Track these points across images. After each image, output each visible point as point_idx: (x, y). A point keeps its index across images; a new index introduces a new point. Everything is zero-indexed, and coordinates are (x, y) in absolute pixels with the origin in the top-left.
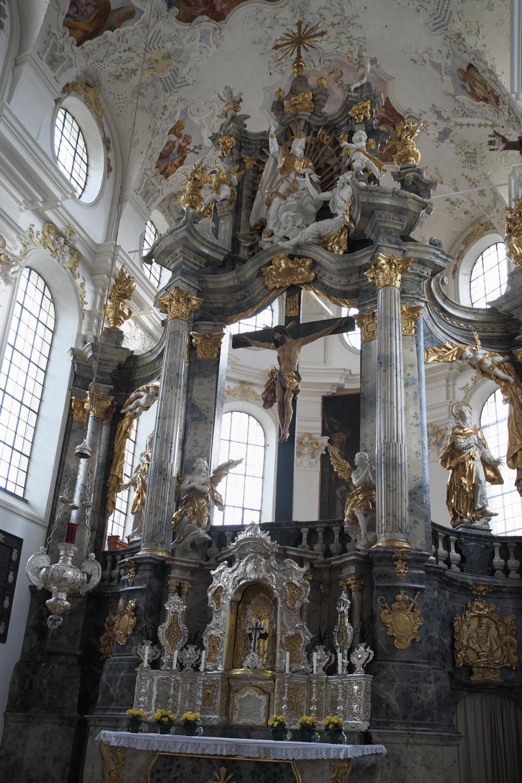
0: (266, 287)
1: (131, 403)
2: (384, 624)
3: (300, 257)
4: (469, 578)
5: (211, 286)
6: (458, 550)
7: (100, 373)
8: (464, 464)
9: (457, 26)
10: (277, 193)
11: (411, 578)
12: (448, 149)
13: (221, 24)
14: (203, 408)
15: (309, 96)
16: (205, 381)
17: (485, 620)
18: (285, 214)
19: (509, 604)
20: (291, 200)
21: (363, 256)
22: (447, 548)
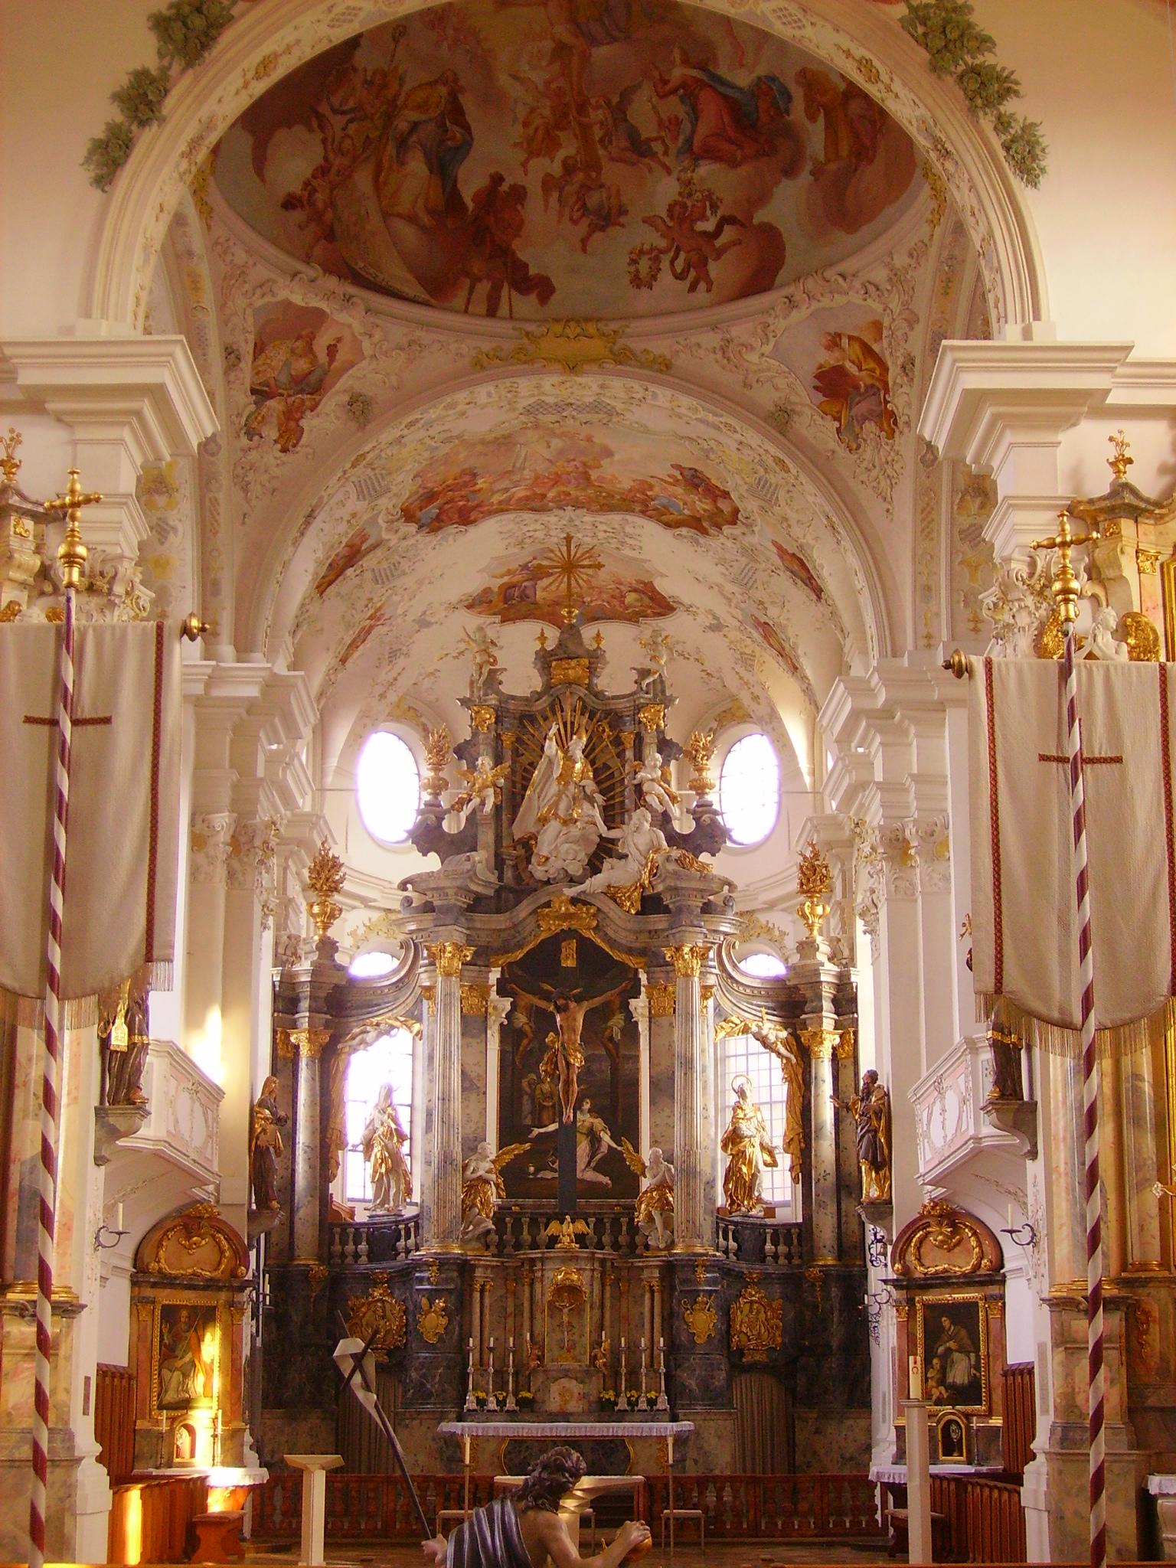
0: (539, 926)
1: (353, 1038)
2: (686, 1323)
3: (585, 903)
4: (743, 1266)
5: (478, 925)
6: (735, 1240)
7: (312, 997)
8: (744, 1152)
9: (759, 594)
10: (556, 815)
11: (708, 1282)
12: (715, 638)
13: (471, 529)
14: (473, 1075)
15: (586, 662)
16: (474, 1042)
17: (755, 1306)
18: (567, 845)
19: (777, 1289)
20: (575, 831)
21: (658, 921)
22: (726, 1238)
